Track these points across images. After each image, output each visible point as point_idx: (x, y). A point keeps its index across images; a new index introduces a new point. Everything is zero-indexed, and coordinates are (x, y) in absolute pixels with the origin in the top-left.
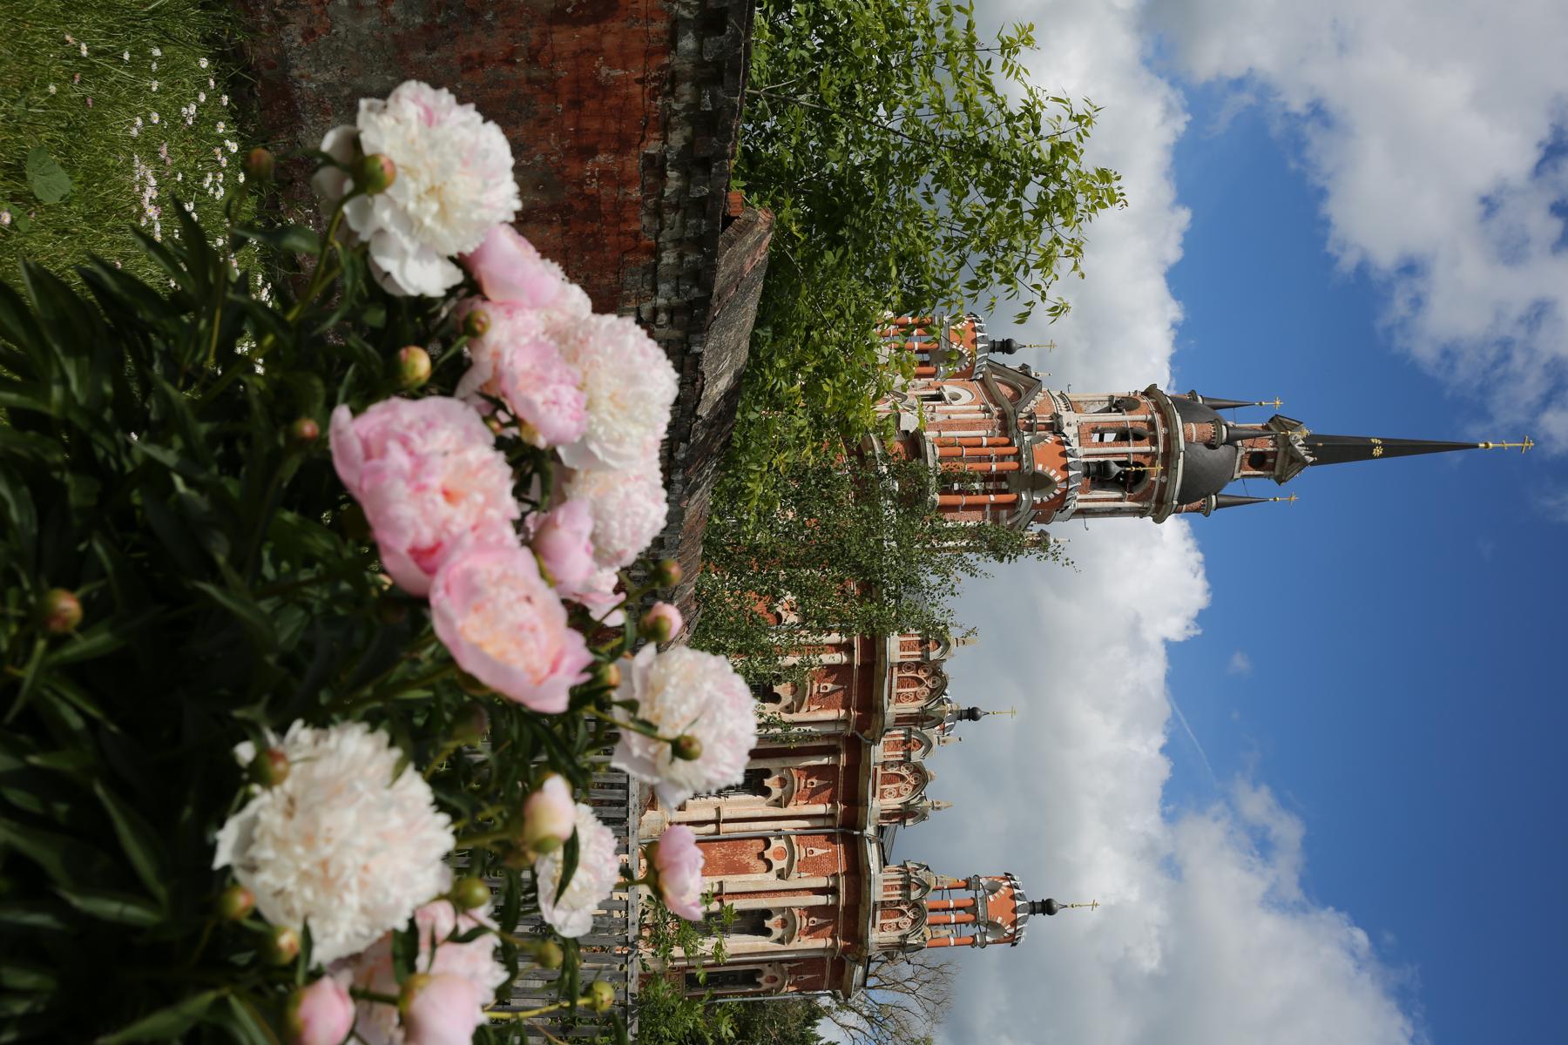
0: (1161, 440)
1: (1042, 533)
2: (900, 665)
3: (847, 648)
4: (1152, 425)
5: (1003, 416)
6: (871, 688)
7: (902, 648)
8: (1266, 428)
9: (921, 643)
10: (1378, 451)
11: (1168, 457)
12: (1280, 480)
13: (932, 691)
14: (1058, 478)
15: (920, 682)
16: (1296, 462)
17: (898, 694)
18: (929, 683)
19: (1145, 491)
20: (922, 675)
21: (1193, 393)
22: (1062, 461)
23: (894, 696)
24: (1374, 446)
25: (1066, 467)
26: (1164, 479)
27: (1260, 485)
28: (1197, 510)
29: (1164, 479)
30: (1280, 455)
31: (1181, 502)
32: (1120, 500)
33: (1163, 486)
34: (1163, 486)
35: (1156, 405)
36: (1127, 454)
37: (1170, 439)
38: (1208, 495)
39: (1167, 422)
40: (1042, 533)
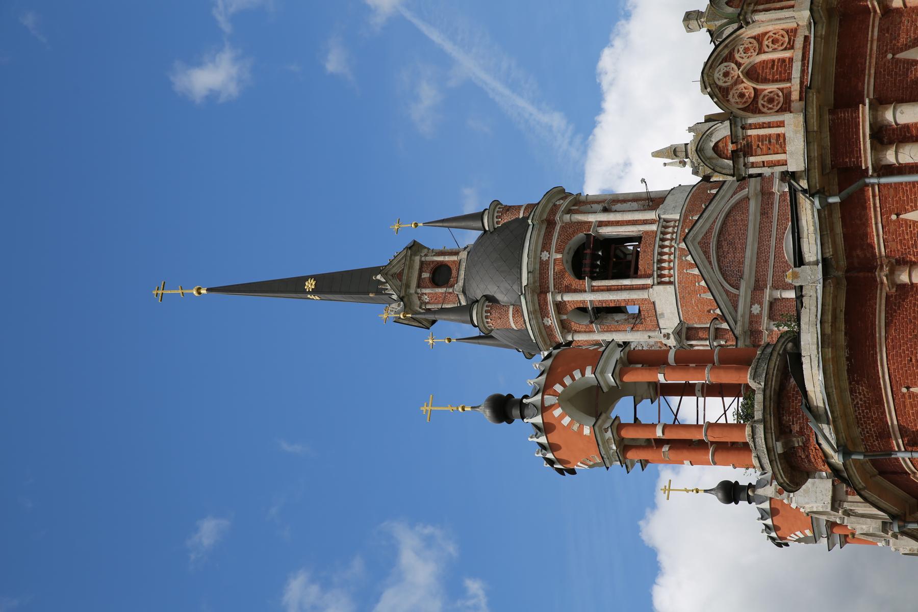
0: (551, 309)
2: (786, 108)
3: (884, 136)
4: (565, 327)
6: (840, 59)
7: (780, 143)
9: (747, 150)
10: (310, 285)
11: (540, 289)
12: (415, 248)
13: (730, 58)
14: (557, 412)
15: (753, 74)
17: (791, 47)
18: (736, 72)
19: (569, 237)
20: (748, 87)
22: (555, 438)
23: (799, 42)
24: (314, 292)
25: (546, 428)
26: (545, 256)
27: (438, 240)
28: (508, 209)
29: (545, 256)
31: (522, 224)
32: (601, 224)
34: (546, 247)
36: (593, 290)
37: (541, 311)
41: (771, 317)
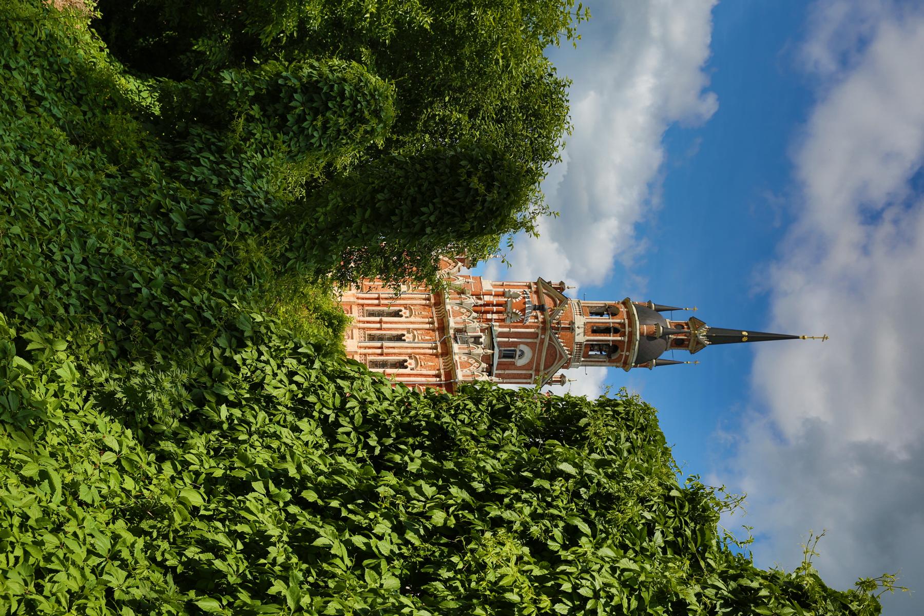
1: (562, 376)
5: (544, 322)
8: (687, 324)
10: (745, 339)
16: (699, 345)
21: (650, 302)
28: (645, 366)
30: (692, 341)
31: (636, 363)
33: (627, 357)
34: (627, 357)
35: (628, 313)
37: (632, 334)
38: (652, 360)
39: (631, 323)
40: (562, 376)
41: (537, 334)
